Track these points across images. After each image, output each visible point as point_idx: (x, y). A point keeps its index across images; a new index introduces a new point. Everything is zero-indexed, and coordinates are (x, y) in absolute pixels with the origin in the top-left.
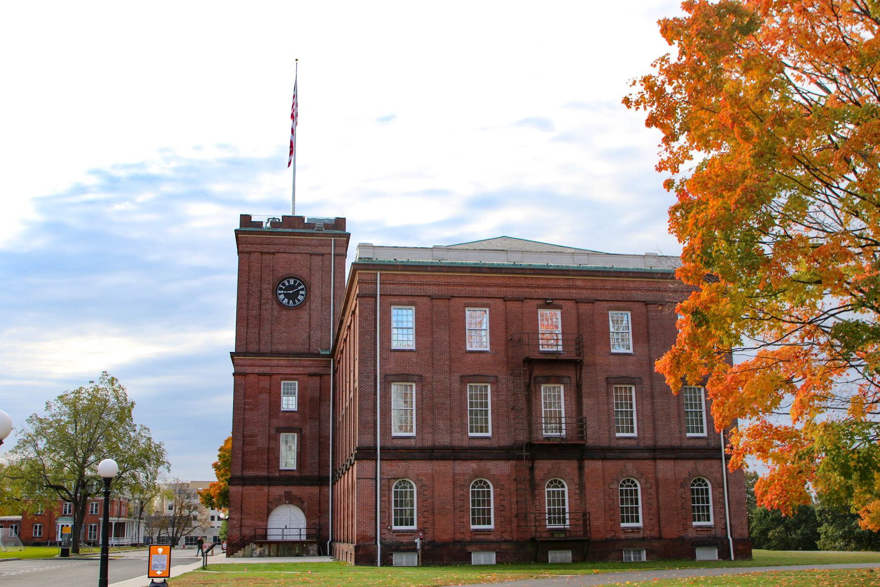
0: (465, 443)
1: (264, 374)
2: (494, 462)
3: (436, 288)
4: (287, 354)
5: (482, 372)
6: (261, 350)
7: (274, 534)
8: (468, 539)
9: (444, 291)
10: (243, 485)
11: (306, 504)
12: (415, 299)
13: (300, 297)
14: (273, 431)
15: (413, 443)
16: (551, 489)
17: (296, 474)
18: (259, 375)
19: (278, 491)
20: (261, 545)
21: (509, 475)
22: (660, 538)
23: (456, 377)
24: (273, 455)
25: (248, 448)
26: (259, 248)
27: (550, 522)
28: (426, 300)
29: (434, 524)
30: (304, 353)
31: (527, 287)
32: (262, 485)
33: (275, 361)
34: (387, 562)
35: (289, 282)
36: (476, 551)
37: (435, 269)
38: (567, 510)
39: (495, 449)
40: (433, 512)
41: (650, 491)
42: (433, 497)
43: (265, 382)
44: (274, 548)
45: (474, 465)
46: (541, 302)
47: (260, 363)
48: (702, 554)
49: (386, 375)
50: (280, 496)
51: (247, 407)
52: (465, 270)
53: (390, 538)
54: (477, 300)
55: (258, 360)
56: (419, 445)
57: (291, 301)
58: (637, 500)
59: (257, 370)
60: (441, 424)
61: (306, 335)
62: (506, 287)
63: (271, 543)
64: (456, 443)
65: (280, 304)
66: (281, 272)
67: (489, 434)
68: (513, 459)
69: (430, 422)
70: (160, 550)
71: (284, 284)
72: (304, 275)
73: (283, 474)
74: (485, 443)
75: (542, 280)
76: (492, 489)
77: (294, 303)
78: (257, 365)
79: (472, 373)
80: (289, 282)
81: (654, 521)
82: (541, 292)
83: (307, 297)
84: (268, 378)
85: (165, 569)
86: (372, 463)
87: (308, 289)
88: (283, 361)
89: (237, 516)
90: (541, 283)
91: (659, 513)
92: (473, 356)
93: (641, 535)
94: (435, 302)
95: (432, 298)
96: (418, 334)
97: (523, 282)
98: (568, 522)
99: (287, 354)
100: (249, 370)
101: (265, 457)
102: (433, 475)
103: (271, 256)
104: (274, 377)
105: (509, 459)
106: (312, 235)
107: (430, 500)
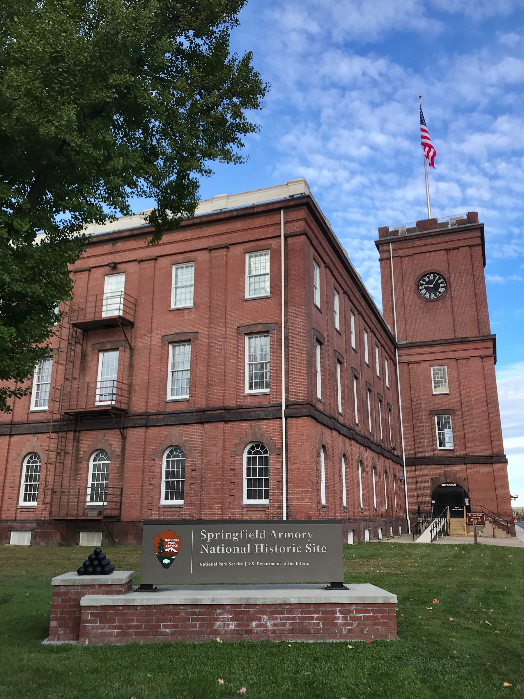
13: (441, 290)
35: (429, 278)
57: (433, 294)
71: (424, 281)
77: (436, 295)
80: (429, 278)
83: (446, 289)
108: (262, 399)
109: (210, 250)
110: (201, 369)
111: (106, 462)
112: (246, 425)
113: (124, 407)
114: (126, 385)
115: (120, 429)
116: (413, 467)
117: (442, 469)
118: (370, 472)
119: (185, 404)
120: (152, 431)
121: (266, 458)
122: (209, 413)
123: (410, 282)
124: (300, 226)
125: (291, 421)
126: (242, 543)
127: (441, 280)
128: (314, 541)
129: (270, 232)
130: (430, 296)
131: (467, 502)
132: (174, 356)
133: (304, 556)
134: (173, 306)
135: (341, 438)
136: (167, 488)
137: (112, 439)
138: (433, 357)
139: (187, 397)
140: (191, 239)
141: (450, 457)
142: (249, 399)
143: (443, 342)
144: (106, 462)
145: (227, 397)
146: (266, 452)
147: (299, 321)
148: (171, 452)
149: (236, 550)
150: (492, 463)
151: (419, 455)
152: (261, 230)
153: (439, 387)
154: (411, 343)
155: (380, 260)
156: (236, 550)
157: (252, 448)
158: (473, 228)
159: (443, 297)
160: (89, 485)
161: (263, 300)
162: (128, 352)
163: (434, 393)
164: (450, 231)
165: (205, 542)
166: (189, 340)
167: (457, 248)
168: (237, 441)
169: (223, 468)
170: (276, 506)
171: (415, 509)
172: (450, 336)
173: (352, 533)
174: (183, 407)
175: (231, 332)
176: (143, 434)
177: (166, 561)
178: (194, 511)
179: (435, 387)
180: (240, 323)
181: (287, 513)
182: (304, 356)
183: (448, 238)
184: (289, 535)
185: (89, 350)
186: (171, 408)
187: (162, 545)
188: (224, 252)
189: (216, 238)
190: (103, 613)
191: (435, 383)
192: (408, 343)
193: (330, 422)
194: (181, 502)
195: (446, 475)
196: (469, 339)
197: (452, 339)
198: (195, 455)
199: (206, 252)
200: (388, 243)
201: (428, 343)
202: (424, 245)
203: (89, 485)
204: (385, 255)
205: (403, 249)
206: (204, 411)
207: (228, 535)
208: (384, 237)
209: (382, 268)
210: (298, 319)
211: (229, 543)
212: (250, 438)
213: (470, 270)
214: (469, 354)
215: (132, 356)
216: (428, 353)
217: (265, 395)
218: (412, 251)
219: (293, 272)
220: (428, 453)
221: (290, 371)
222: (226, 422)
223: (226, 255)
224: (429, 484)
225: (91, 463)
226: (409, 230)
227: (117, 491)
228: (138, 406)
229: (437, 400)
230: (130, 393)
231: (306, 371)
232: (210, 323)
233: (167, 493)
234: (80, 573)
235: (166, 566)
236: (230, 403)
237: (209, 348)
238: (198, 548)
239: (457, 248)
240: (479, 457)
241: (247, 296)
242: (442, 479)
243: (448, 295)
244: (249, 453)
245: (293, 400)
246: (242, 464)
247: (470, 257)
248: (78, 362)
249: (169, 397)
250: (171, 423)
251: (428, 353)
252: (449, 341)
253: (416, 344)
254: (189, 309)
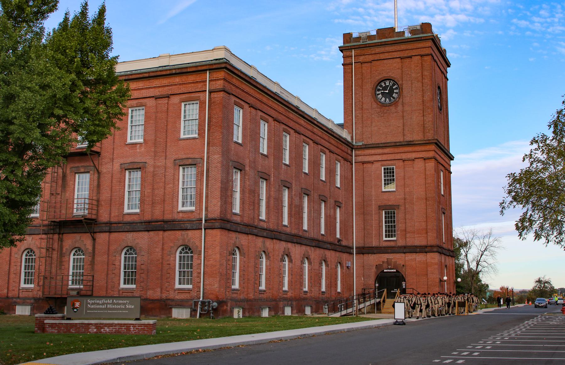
13: (394, 95)
27: (73, 283)
35: (385, 84)
57: (387, 99)
71: (381, 86)
77: (390, 100)
80: (385, 84)
87: (400, 88)
108: (190, 215)
109: (157, 98)
110: (148, 191)
111: (82, 257)
112: (179, 233)
113: (94, 217)
114: (95, 202)
115: (91, 233)
116: (362, 255)
117: (385, 257)
118: (298, 263)
119: (137, 216)
120: (114, 235)
121: (192, 257)
122: (153, 223)
123: (369, 87)
124: (220, 84)
125: (209, 231)
126: (103, 304)
127: (396, 86)
128: (130, 304)
129: (199, 87)
131: (404, 285)
132: (130, 179)
133: (126, 309)
134: (129, 141)
135: (261, 239)
136: (125, 276)
137: (85, 240)
138: (385, 157)
139: (138, 211)
140: (142, 89)
141: (393, 247)
142: (181, 215)
143: (393, 144)
144: (82, 257)
145: (166, 212)
146: (192, 253)
147: (217, 158)
148: (128, 251)
149: (101, 306)
150: (426, 252)
151: (367, 245)
152: (193, 85)
153: (388, 184)
154: (365, 145)
155: (343, 65)
156: (101, 306)
157: (183, 249)
158: (425, 38)
160: (71, 273)
161: (193, 140)
162: (96, 175)
163: (383, 190)
164: (405, 41)
165: (89, 304)
166: (140, 168)
167: (411, 57)
168: (172, 245)
169: (162, 263)
170: (196, 289)
171: (360, 292)
172: (400, 139)
173: (267, 310)
174: (136, 218)
175: (170, 164)
176: (108, 237)
177: (75, 310)
178: (143, 292)
179: (385, 184)
180: (176, 157)
181: (203, 294)
182: (219, 185)
183: (403, 47)
184: (120, 302)
185: (68, 172)
186: (128, 219)
187: (74, 304)
188: (165, 101)
189: (160, 89)
190: (52, 325)
191: (385, 180)
192: (363, 145)
193: (247, 230)
194: (134, 286)
195: (388, 262)
196: (414, 143)
197: (400, 142)
198: (143, 253)
199: (154, 99)
200: (350, 49)
201: (381, 145)
202: (382, 53)
203: (71, 273)
204: (348, 61)
205: (364, 55)
206: (149, 222)
207: (98, 301)
208: (348, 43)
209: (345, 72)
210: (216, 156)
211: (98, 304)
212: (181, 242)
213: (420, 78)
214: (414, 155)
215: (99, 178)
216: (379, 154)
217: (192, 212)
218: (371, 58)
219: (214, 120)
220: (374, 244)
221: (209, 195)
222: (164, 231)
223: (168, 103)
224: (374, 269)
225: (72, 257)
226: (370, 37)
227: (90, 278)
228: (104, 217)
229: (385, 196)
230: (98, 206)
231: (219, 196)
232: (155, 156)
233: (125, 279)
234: (45, 313)
235: (75, 312)
236: (168, 217)
237: (154, 175)
238: (87, 306)
239: (411, 57)
240: (416, 247)
241: (182, 136)
242: (385, 265)
243: (401, 100)
244: (181, 253)
245: (210, 216)
246: (175, 261)
247: (420, 66)
248: (60, 182)
249: (126, 211)
250: (127, 230)
251: (379, 154)
252: (398, 144)
253: (370, 146)
254: (140, 144)
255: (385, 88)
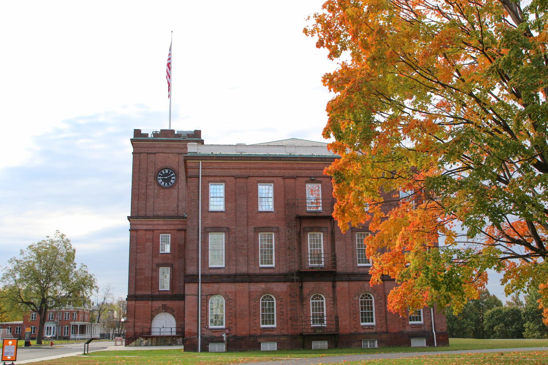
0: (257, 272)
1: (149, 230)
2: (276, 284)
3: (239, 171)
4: (164, 217)
5: (269, 225)
6: (147, 215)
7: (155, 332)
8: (259, 334)
9: (244, 173)
10: (136, 300)
11: (175, 312)
12: (224, 178)
13: (172, 181)
14: (155, 266)
15: (223, 271)
16: (314, 301)
17: (170, 293)
18: (146, 230)
19: (158, 304)
20: (146, 338)
21: (286, 292)
22: (387, 332)
23: (251, 228)
24: (154, 280)
25: (139, 277)
26: (146, 150)
28: (232, 179)
29: (236, 325)
30: (174, 216)
31: (298, 169)
32: (148, 300)
33: (156, 221)
34: (205, 349)
35: (165, 171)
36: (264, 342)
37: (237, 159)
38: (325, 315)
39: (277, 275)
40: (236, 317)
41: (380, 301)
42: (235, 307)
43: (149, 235)
44: (154, 340)
45: (263, 286)
46: (308, 179)
47: (146, 223)
48: (415, 343)
49: (205, 228)
50: (159, 307)
51: (138, 251)
52: (258, 159)
53: (208, 334)
54: (265, 179)
55: (144, 221)
56: (227, 273)
58: (372, 307)
59: (145, 227)
60: (241, 259)
61: (175, 205)
62: (284, 169)
63: (153, 337)
64: (251, 271)
65: (159, 185)
66: (160, 166)
67: (273, 265)
68: (289, 282)
69: (234, 258)
70: (10, 342)
71: (162, 173)
72: (175, 167)
73: (161, 293)
74: (271, 271)
75: (309, 165)
76: (275, 301)
77: (168, 184)
78: (144, 224)
79: (262, 226)
80: (165, 171)
81: (384, 321)
82: (308, 173)
83: (176, 181)
84: (151, 232)
85: (13, 355)
86: (196, 285)
87: (177, 176)
88: (161, 222)
89: (132, 320)
90: (308, 166)
91: (386, 316)
92: (263, 215)
93: (374, 330)
94: (238, 180)
95: (236, 177)
96: (227, 201)
97: (296, 166)
98: (325, 322)
99: (164, 217)
100: (140, 227)
101: (150, 282)
102: (236, 292)
103: (154, 155)
104: (155, 232)
105: (285, 282)
106: (180, 141)
107: (234, 309)
130: (165, 184)
159: (173, 186)
255: (166, 175)
